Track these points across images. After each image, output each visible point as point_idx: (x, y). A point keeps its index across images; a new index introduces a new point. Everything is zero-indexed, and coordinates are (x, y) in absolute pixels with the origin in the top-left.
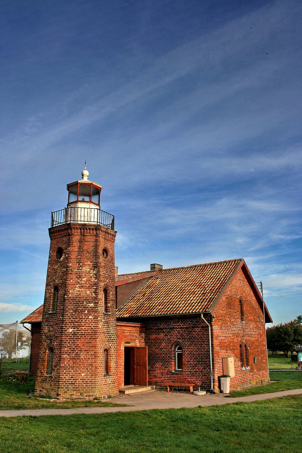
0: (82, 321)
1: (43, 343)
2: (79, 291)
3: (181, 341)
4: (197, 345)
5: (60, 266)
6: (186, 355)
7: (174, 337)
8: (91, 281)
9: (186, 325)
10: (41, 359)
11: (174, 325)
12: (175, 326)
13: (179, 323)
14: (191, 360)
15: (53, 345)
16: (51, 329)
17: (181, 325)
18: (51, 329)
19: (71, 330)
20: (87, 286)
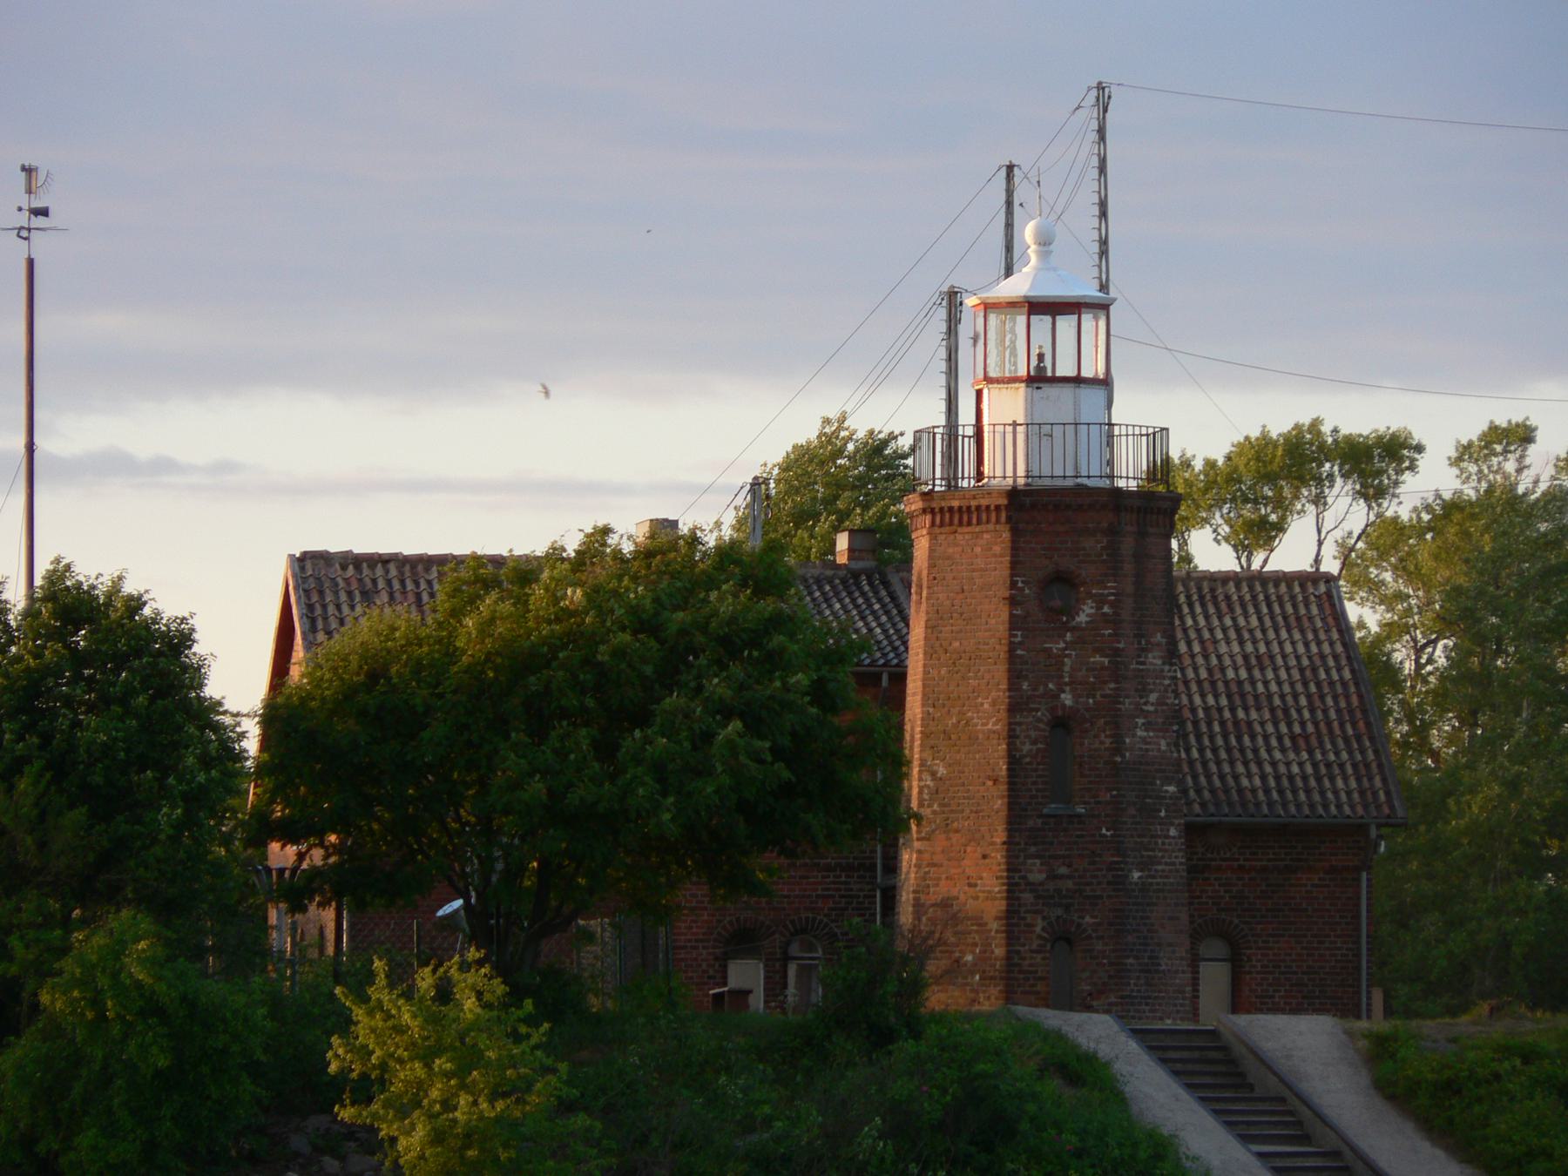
0: (1156, 843)
1: (1024, 919)
2: (1144, 740)
3: (1236, 921)
4: (1305, 936)
5: (1071, 642)
6: (1258, 973)
7: (1207, 903)
8: (1167, 704)
9: (1261, 860)
10: (1020, 972)
11: (1209, 856)
12: (1215, 860)
13: (1230, 850)
14: (1280, 991)
15: (1079, 925)
16: (1063, 870)
17: (1238, 860)
18: (1063, 870)
19: (1136, 875)
20: (1160, 720)
